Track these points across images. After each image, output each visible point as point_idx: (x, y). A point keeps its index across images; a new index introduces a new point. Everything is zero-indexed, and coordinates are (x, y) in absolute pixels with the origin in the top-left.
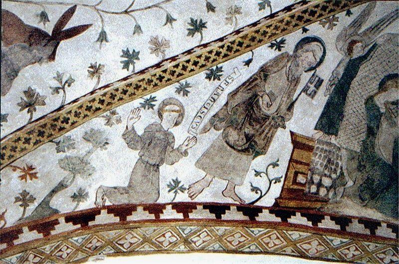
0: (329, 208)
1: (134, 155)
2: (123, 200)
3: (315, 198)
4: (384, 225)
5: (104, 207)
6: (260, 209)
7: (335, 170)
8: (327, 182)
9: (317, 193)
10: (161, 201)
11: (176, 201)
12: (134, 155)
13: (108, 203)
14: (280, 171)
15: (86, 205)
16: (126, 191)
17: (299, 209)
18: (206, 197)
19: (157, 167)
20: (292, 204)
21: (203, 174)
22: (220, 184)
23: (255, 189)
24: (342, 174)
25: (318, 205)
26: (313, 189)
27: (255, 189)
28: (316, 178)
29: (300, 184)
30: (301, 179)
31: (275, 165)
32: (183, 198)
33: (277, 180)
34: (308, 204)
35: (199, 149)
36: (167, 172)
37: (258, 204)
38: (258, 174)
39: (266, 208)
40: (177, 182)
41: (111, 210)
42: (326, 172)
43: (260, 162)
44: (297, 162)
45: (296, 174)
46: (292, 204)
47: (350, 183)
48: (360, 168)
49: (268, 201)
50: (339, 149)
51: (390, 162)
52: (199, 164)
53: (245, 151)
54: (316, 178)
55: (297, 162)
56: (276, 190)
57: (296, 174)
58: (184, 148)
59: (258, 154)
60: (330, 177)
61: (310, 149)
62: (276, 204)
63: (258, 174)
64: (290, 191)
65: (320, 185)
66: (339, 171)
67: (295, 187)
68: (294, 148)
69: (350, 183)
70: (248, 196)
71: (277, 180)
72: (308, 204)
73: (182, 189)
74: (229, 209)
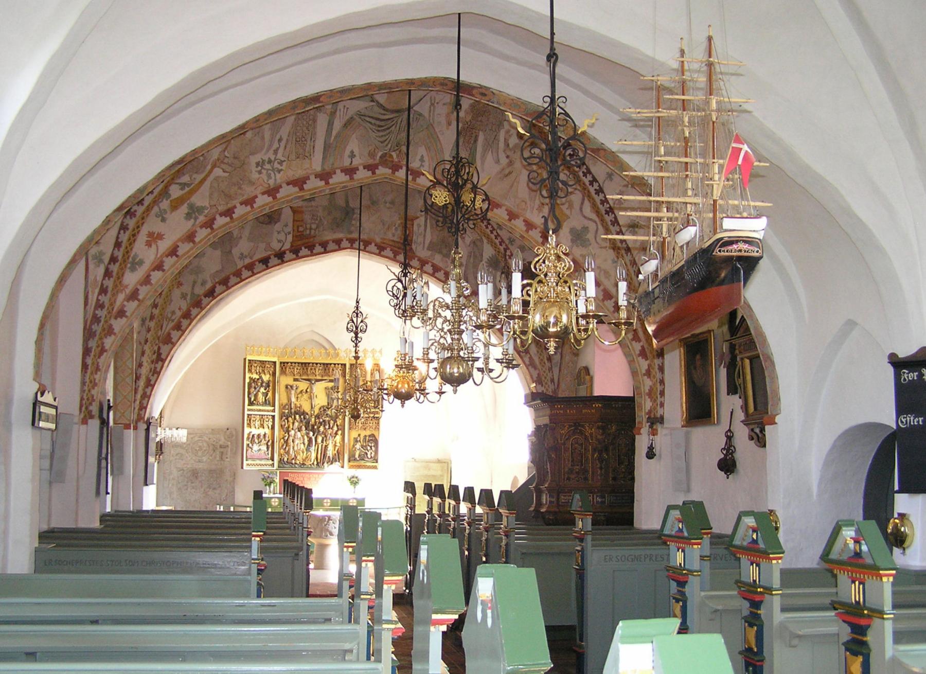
0: (317, 239)
1: (218, 253)
2: (223, 275)
3: (309, 236)
4: (344, 240)
5: (216, 283)
6: (284, 253)
7: (317, 219)
8: (314, 226)
9: (310, 234)
10: (239, 267)
11: (245, 264)
12: (218, 253)
13: (217, 280)
14: (289, 229)
15: (209, 285)
16: (222, 271)
17: (303, 245)
18: (258, 256)
19: (230, 252)
20: (299, 243)
21: (252, 244)
22: (262, 246)
23: (279, 241)
24: (321, 219)
25: (312, 240)
26: (308, 232)
27: (279, 241)
28: (308, 226)
29: (301, 232)
30: (301, 229)
31: (286, 225)
32: (247, 261)
33: (289, 233)
34: (307, 241)
35: (246, 233)
36: (236, 252)
37: (283, 249)
38: (279, 233)
39: (287, 250)
40: (242, 254)
41: (220, 283)
42: (313, 221)
43: (278, 226)
44: (297, 221)
45: (298, 227)
46: (299, 243)
47: (326, 223)
48: (329, 214)
49: (287, 246)
50: (317, 207)
51: (344, 205)
52: (250, 239)
53: (270, 223)
54: (308, 226)
55: (297, 221)
56: (290, 238)
57: (298, 227)
58: (239, 236)
59: (276, 223)
60: (315, 223)
61: (302, 212)
62: (292, 246)
63: (279, 233)
64: (296, 236)
65: (311, 229)
66: (319, 219)
67: (299, 234)
68: (294, 214)
69: (326, 223)
70: (276, 246)
71: (289, 233)
72: (307, 241)
73: (246, 257)
74: (270, 258)
